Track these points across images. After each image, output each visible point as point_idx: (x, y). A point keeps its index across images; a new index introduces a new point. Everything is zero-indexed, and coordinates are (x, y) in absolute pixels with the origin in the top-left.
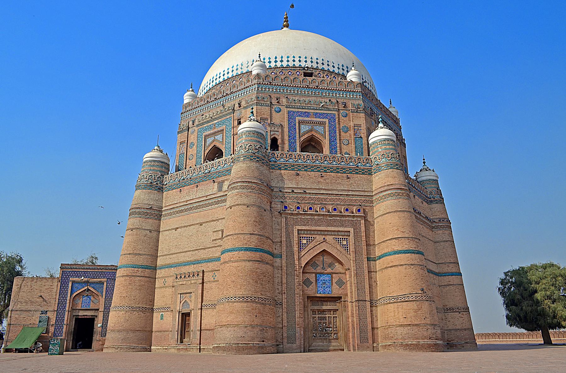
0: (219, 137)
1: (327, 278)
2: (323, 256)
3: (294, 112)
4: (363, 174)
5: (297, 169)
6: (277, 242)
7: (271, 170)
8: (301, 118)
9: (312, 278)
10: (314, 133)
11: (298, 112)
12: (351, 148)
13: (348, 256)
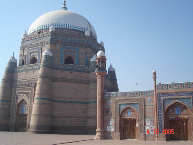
10: (34, 56)
11: (30, 49)
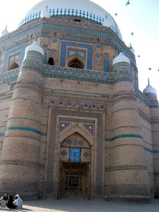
0: (17, 57)
1: (78, 151)
2: (76, 136)
3: (65, 42)
4: (107, 83)
5: (62, 77)
6: (45, 125)
7: (45, 77)
8: (69, 47)
9: (67, 150)
10: (78, 57)
11: (68, 43)
12: (101, 67)
13: (93, 137)
